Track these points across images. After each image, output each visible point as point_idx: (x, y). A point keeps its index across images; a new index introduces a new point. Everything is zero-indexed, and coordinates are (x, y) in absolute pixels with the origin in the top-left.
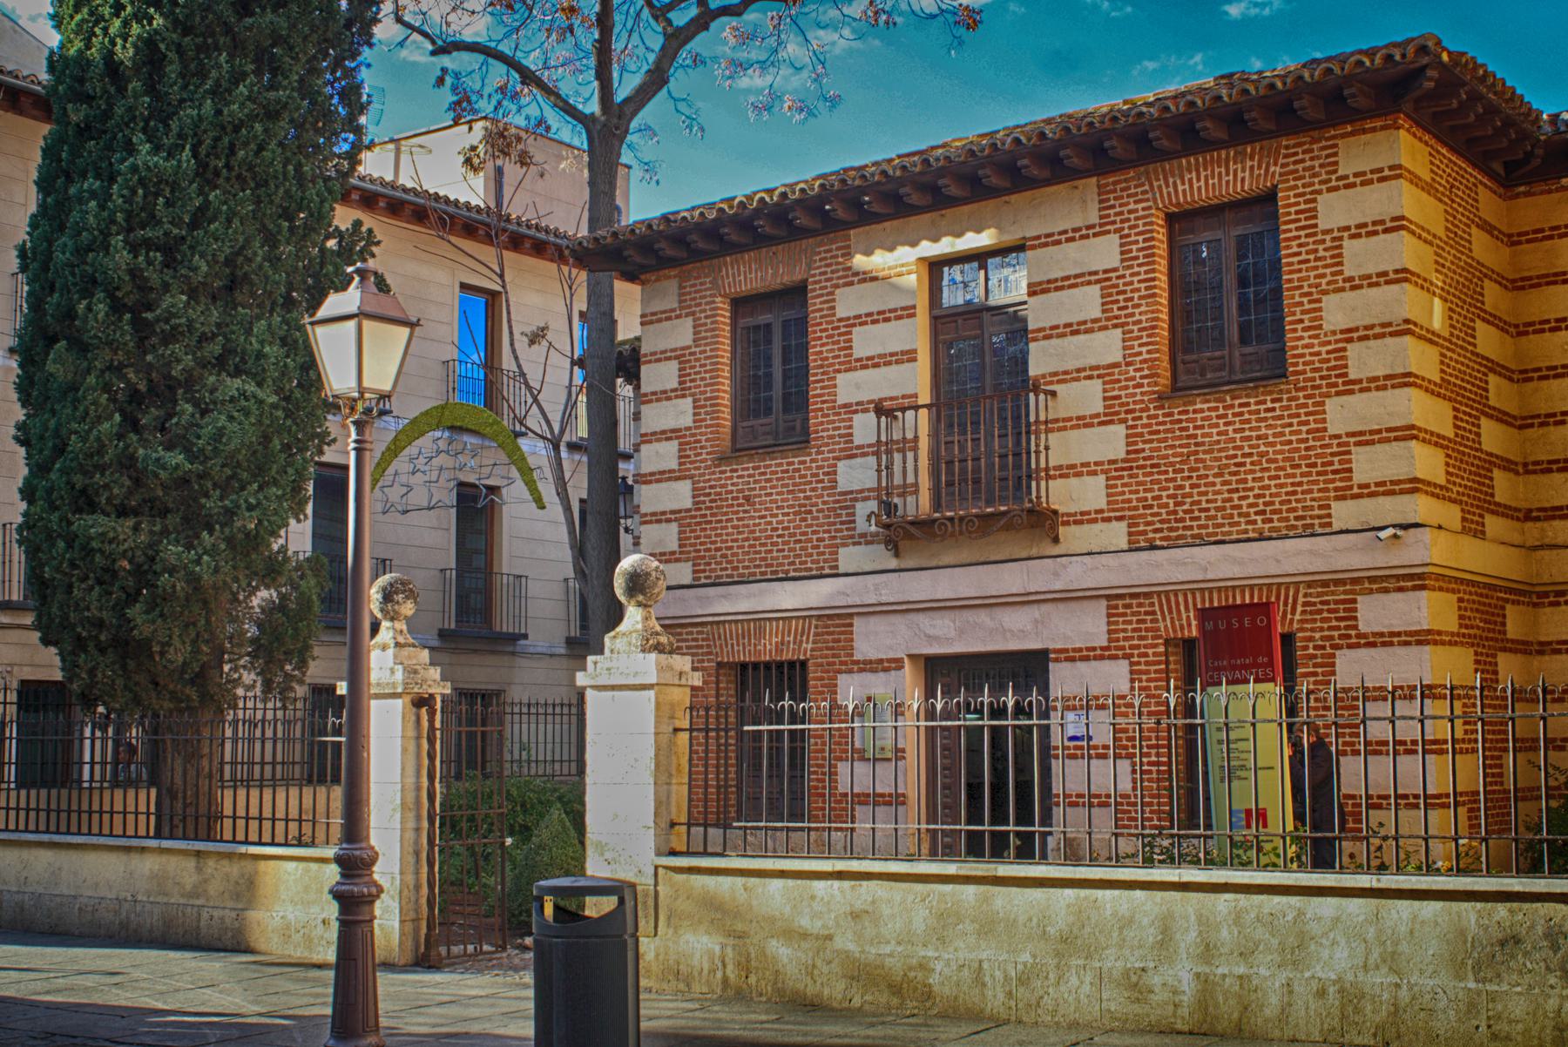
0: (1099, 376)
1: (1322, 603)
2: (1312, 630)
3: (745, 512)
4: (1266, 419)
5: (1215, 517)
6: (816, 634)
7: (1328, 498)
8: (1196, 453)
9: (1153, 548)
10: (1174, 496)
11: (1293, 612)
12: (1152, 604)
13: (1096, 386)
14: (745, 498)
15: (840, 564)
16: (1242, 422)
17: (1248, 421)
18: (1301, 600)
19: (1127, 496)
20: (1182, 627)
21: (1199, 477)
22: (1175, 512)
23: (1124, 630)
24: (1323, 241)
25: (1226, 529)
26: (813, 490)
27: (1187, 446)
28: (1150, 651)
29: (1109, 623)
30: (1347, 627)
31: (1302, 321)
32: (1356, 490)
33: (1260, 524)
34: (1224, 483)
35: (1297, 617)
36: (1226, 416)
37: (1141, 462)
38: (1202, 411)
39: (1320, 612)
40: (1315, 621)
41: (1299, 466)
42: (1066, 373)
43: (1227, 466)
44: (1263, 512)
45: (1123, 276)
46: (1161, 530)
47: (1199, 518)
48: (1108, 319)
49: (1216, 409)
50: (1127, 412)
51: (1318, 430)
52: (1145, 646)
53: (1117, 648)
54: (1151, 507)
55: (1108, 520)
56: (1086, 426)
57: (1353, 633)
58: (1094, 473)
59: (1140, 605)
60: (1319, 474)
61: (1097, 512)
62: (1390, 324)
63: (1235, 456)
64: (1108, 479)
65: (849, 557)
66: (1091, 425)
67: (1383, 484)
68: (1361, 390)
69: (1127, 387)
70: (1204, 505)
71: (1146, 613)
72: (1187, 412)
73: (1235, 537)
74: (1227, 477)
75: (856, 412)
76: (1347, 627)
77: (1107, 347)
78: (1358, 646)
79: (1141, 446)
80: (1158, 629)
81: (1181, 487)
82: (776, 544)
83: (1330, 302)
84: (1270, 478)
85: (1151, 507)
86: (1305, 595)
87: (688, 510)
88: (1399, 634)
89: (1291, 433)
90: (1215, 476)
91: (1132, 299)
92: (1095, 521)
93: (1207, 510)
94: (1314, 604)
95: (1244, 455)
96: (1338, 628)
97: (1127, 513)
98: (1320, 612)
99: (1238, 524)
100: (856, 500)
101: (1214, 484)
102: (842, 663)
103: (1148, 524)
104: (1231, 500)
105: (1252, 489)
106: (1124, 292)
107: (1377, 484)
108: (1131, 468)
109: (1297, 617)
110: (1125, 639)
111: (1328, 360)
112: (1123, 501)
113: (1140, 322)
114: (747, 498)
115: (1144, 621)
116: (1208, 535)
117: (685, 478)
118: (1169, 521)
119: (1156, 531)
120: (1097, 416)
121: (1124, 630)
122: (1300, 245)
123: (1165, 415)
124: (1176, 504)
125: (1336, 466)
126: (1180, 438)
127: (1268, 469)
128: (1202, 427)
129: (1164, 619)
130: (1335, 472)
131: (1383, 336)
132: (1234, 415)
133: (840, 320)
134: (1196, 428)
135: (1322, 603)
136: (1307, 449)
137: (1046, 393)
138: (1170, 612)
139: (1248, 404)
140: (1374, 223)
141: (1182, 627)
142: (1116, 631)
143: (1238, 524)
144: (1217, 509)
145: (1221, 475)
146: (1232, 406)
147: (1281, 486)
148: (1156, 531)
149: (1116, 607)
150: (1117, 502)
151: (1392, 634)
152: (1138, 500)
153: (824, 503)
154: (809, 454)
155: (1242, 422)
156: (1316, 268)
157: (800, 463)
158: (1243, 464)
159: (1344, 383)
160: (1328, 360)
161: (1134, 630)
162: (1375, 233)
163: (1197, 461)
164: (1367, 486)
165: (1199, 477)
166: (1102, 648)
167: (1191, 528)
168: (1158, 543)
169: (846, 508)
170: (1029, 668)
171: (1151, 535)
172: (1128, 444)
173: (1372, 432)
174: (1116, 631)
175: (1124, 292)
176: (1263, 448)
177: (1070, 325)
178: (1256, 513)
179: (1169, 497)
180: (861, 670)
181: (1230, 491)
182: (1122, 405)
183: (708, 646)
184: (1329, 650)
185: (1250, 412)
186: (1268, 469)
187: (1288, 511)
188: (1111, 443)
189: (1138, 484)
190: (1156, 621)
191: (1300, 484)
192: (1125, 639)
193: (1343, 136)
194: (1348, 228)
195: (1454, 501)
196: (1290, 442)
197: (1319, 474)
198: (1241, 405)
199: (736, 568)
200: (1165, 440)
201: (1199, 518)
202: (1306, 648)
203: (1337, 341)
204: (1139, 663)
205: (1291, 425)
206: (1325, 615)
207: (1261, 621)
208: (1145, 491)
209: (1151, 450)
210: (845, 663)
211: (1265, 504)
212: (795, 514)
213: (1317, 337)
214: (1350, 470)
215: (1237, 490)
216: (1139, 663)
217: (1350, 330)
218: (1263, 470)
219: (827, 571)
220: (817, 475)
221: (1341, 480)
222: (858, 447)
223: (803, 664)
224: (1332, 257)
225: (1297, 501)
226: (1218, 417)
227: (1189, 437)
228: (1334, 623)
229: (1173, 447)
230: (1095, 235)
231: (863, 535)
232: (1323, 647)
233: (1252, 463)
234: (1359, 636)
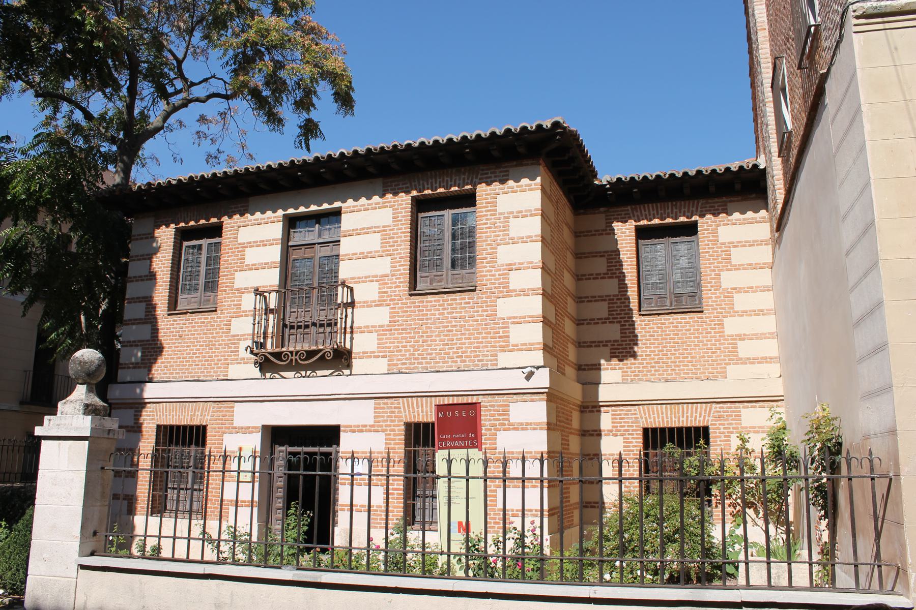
0: (377, 281)
1: (490, 406)
4: (465, 308)
5: (435, 358)
6: (213, 412)
9: (400, 373)
10: (413, 346)
12: (399, 403)
13: (376, 285)
15: (229, 374)
16: (452, 309)
17: (456, 308)
20: (414, 416)
21: (427, 337)
22: (414, 355)
23: (383, 417)
24: (499, 219)
25: (441, 364)
26: (217, 333)
27: (422, 319)
28: (396, 428)
30: (503, 419)
31: (486, 258)
33: (459, 363)
36: (443, 305)
38: (431, 302)
41: (481, 333)
42: (359, 278)
43: (443, 331)
45: (393, 230)
46: (405, 364)
47: (426, 358)
48: (383, 251)
49: (439, 301)
50: (391, 300)
51: (492, 315)
52: (394, 426)
53: (379, 426)
54: (401, 351)
55: (378, 357)
56: (368, 306)
58: (371, 332)
59: (392, 403)
60: (492, 338)
61: (371, 352)
62: (532, 263)
63: (448, 326)
65: (235, 371)
66: (371, 306)
67: (525, 344)
68: (516, 296)
69: (391, 287)
70: (430, 351)
71: (395, 408)
72: (423, 302)
73: (445, 369)
74: (443, 337)
75: (244, 293)
76: (503, 419)
77: (383, 266)
78: (508, 429)
79: (397, 318)
80: (401, 417)
81: (417, 341)
82: (195, 361)
83: (501, 250)
84: (466, 339)
85: (401, 351)
87: (148, 341)
88: (531, 424)
89: (478, 316)
90: (436, 336)
91: (397, 242)
92: (370, 357)
93: (431, 354)
95: (452, 326)
98: (490, 410)
99: (447, 362)
100: (240, 340)
101: (435, 341)
102: (226, 428)
103: (398, 360)
105: (456, 344)
106: (393, 238)
107: (522, 345)
111: (499, 279)
113: (400, 254)
115: (393, 412)
116: (431, 367)
117: (147, 323)
118: (410, 359)
119: (403, 364)
120: (375, 301)
121: (383, 417)
122: (487, 219)
123: (411, 303)
124: (415, 350)
125: (501, 334)
126: (419, 315)
127: (464, 334)
128: (431, 310)
130: (500, 337)
131: (528, 268)
132: (448, 305)
133: (240, 244)
134: (427, 310)
135: (490, 406)
136: (486, 324)
137: (348, 287)
139: (455, 300)
140: (526, 211)
141: (414, 416)
143: (447, 362)
144: (437, 354)
145: (440, 336)
147: (471, 343)
148: (403, 364)
151: (527, 424)
152: (394, 347)
153: (223, 340)
155: (452, 309)
156: (495, 232)
158: (452, 331)
160: (499, 279)
161: (388, 417)
162: (526, 216)
163: (427, 328)
164: (517, 345)
165: (427, 337)
167: (422, 363)
168: (403, 370)
169: (234, 344)
170: (330, 434)
172: (391, 317)
173: (521, 317)
175: (393, 238)
176: (462, 323)
177: (363, 253)
178: (457, 357)
181: (444, 345)
182: (388, 296)
185: (456, 304)
186: (464, 334)
187: (475, 356)
188: (381, 316)
189: (394, 338)
190: (401, 412)
191: (481, 343)
193: (512, 166)
194: (512, 213)
195: (555, 356)
196: (477, 321)
197: (492, 338)
198: (452, 300)
199: (172, 373)
200: (410, 316)
201: (426, 358)
203: (504, 270)
204: (390, 435)
205: (478, 311)
207: (472, 413)
208: (398, 342)
210: (228, 428)
211: (463, 352)
213: (493, 267)
214: (508, 337)
215: (447, 344)
216: (390, 435)
217: (511, 264)
218: (462, 334)
219: (222, 378)
220: (220, 325)
221: (504, 341)
222: (243, 312)
223: (205, 427)
224: (504, 226)
225: (480, 351)
226: (439, 305)
227: (423, 315)
230: (380, 208)
231: (243, 359)
232: (490, 430)
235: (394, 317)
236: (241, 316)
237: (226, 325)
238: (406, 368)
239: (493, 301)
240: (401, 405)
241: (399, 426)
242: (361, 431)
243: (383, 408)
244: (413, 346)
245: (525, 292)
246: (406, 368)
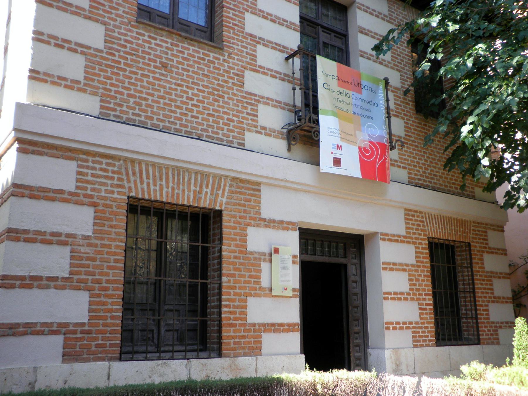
3: (163, 75)
6: (231, 192)
14: (161, 63)
26: (226, 82)
100: (259, 101)
102: (251, 218)
109: (471, 236)
114: (164, 66)
153: (234, 94)
154: (223, 55)
157: (214, 57)
180: (266, 226)
183: (119, 179)
210: (254, 219)
212: (209, 93)
219: (235, 145)
236: (258, 71)
237: (237, 75)
240: (424, 220)
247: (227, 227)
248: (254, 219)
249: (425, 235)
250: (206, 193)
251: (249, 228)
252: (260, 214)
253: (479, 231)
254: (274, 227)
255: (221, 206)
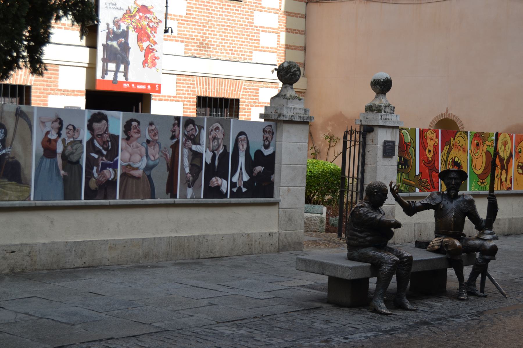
2: (246, 99)
4: (235, 13)
7: (252, 49)
8: (211, 21)
10: (202, 37)
11: (240, 91)
18: (243, 87)
19: (185, 33)
23: (183, 90)
27: (208, 17)
29: (177, 86)
32: (260, 48)
34: (220, 36)
35: (241, 93)
37: (191, 19)
39: (248, 92)
40: (246, 95)
44: (232, 50)
52: (190, 98)
53: (180, 97)
54: (194, 39)
57: (257, 101)
59: (189, 80)
64: (178, 23)
71: (191, 84)
74: (221, 33)
79: (192, 12)
80: (195, 91)
81: (205, 34)
85: (194, 39)
86: (245, 85)
94: (247, 89)
96: (253, 99)
97: (185, 40)
98: (248, 92)
101: (216, 35)
102: (51, 90)
103: (193, 46)
104: (222, 43)
108: (187, 21)
109: (241, 93)
110: (183, 94)
112: (184, 34)
121: (183, 90)
129: (198, 88)
138: (200, 85)
142: (179, 90)
144: (217, 46)
146: (225, 5)
147: (238, 41)
149: (180, 80)
150: (181, 34)
159: (261, 7)
164: (263, 48)
165: (212, 31)
166: (174, 97)
171: (193, 51)
174: (179, 90)
179: (200, 36)
184: (249, 107)
192: (183, 94)
202: (243, 105)
204: (187, 105)
206: (250, 93)
209: (196, 15)
210: (53, 90)
211: (233, 47)
215: (224, 39)
216: (187, 105)
228: (252, 97)
229: (203, 16)
233: (230, 30)
234: (259, 103)
235: (190, 10)
238: (198, 54)
239: (252, 13)
240: (195, 82)
241: (193, 98)
242: (167, 100)
243: (183, 83)
244: (202, 37)
245: (272, 10)
246: (198, 54)
247: (35, 96)
248: (53, 90)
249: (193, 95)
250: (21, 75)
251: (49, 96)
252: (57, 86)
253: (250, 89)
254: (68, 95)
255: (31, 83)
